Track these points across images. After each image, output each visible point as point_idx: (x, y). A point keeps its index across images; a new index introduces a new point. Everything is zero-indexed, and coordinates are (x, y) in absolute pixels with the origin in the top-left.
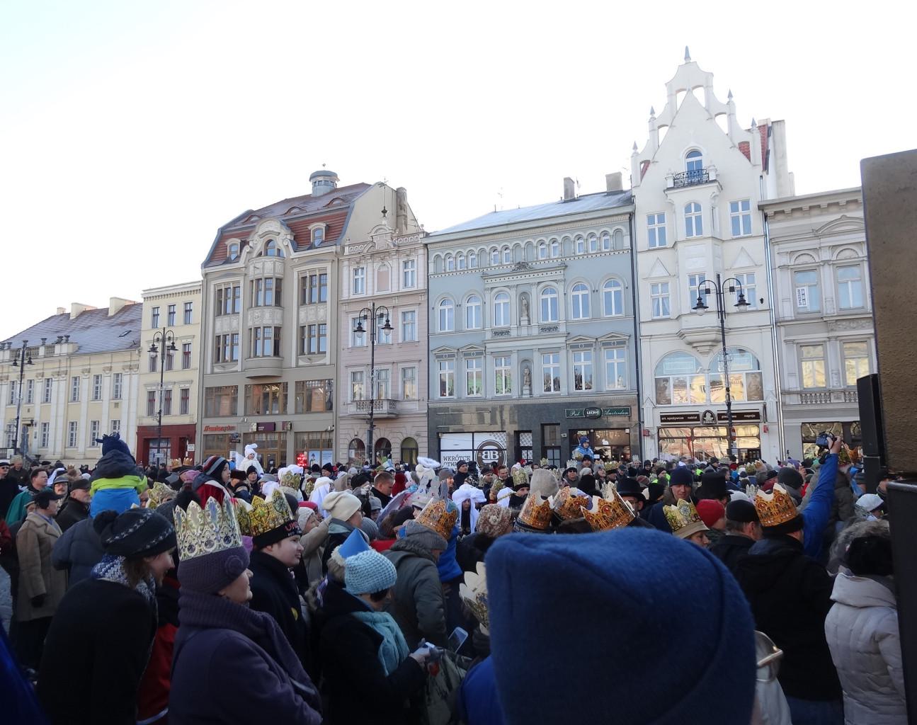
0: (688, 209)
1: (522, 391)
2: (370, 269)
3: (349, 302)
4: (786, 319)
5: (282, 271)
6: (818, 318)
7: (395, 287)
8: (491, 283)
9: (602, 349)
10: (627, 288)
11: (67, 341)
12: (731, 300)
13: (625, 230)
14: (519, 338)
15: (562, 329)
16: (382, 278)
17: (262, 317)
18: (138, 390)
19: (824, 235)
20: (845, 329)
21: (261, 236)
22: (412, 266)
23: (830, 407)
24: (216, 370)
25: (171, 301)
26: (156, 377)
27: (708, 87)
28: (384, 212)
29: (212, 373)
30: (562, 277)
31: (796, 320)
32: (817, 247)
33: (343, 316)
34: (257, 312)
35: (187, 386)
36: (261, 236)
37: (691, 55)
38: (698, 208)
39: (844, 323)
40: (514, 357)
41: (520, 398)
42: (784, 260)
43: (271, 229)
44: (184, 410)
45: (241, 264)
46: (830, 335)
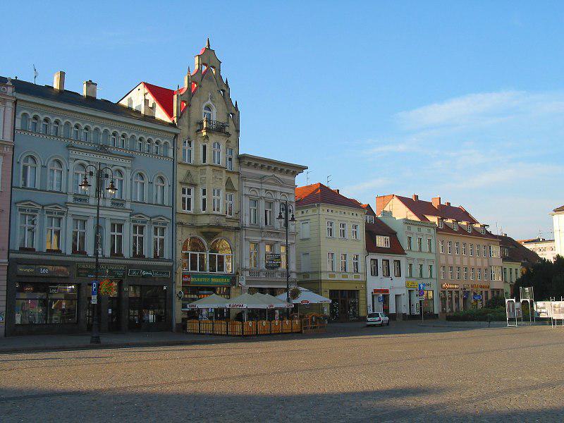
8: (74, 154)
13: (170, 144)
15: (128, 206)
19: (265, 183)
30: (129, 166)
38: (219, 145)
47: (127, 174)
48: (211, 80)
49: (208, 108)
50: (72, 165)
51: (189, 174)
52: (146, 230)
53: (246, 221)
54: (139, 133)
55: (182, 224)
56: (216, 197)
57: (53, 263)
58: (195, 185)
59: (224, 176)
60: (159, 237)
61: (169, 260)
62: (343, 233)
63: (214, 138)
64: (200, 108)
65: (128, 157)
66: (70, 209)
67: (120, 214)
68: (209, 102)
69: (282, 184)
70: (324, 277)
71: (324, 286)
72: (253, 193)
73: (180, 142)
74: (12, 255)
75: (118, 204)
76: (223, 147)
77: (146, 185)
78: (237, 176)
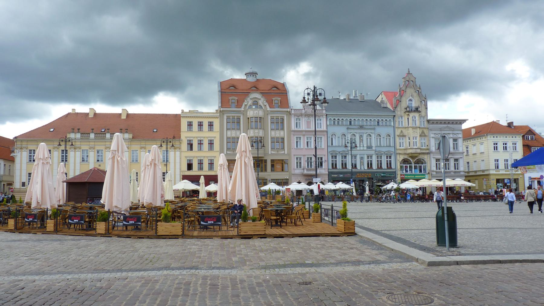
0: (413, 117)
2: (303, 120)
3: (294, 131)
8: (350, 131)
11: (127, 132)
13: (392, 120)
15: (374, 148)
17: (259, 133)
18: (180, 158)
24: (228, 152)
25: (200, 120)
33: (292, 135)
34: (256, 131)
38: (415, 118)
42: (433, 135)
45: (242, 109)
47: (373, 135)
48: (411, 88)
49: (411, 100)
51: (402, 131)
52: (383, 157)
53: (433, 149)
56: (415, 140)
58: (405, 136)
59: (419, 131)
60: (389, 160)
62: (505, 148)
63: (412, 115)
64: (406, 101)
68: (411, 98)
69: (453, 130)
70: (491, 172)
71: (492, 177)
73: (396, 118)
75: (369, 147)
76: (417, 118)
77: (382, 139)
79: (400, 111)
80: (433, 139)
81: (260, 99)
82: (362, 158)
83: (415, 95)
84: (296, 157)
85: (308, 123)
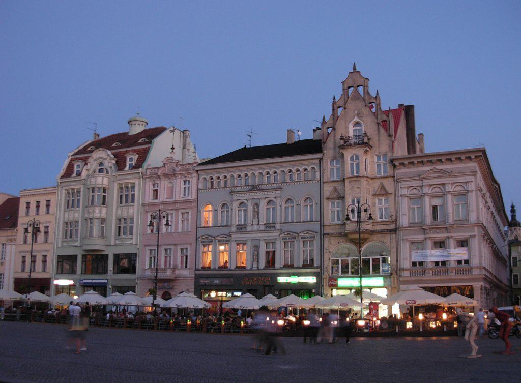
0: (352, 159)
1: (252, 265)
4: (404, 226)
5: (107, 183)
6: (419, 227)
7: (179, 196)
8: (236, 197)
9: (301, 240)
10: (317, 204)
12: (364, 215)
13: (317, 169)
14: (252, 232)
15: (278, 227)
16: (171, 191)
17: (93, 211)
20: (434, 233)
21: (95, 160)
22: (189, 184)
23: (425, 278)
25: (38, 198)
26: (28, 247)
27: (365, 87)
28: (173, 148)
29: (63, 246)
30: (279, 195)
31: (409, 227)
32: (421, 185)
35: (45, 254)
36: (95, 160)
37: (357, 67)
38: (357, 158)
39: (433, 230)
40: (249, 243)
41: (251, 269)
43: (102, 156)
44: (44, 269)
46: (427, 236)
47: (278, 202)
49: (357, 124)
50: (235, 205)
51: (335, 190)
53: (404, 221)
54: (250, 170)
55: (328, 234)
57: (223, 276)
60: (309, 249)
61: (317, 267)
65: (277, 189)
66: (233, 236)
67: (271, 234)
68: (356, 119)
72: (459, 188)
74: (198, 272)
78: (392, 179)
79: (329, 151)
80: (406, 200)
81: (105, 159)
82: (256, 248)
83: (365, 111)
84: (147, 249)
85: (171, 191)
